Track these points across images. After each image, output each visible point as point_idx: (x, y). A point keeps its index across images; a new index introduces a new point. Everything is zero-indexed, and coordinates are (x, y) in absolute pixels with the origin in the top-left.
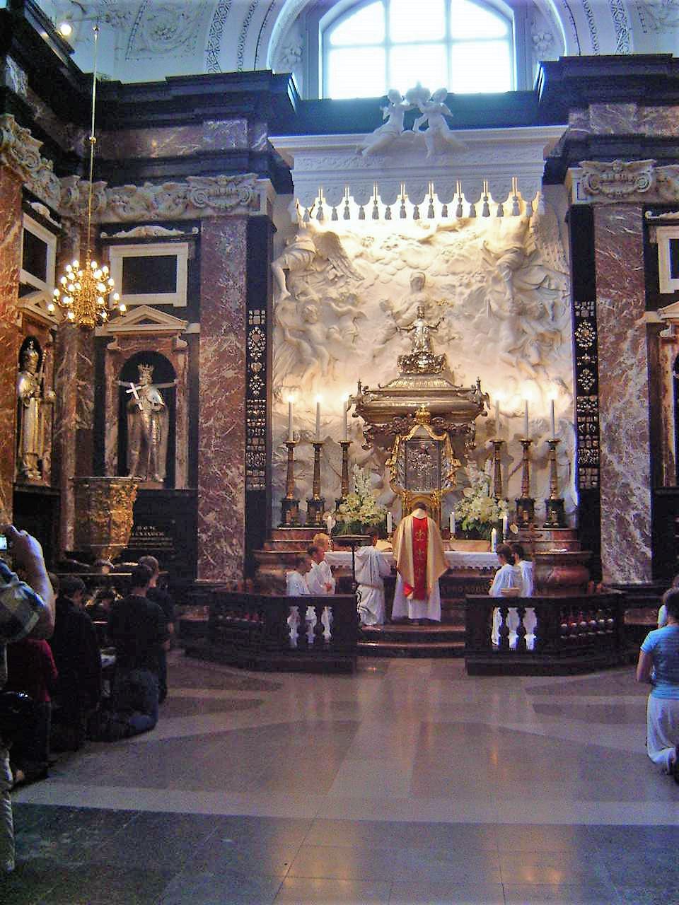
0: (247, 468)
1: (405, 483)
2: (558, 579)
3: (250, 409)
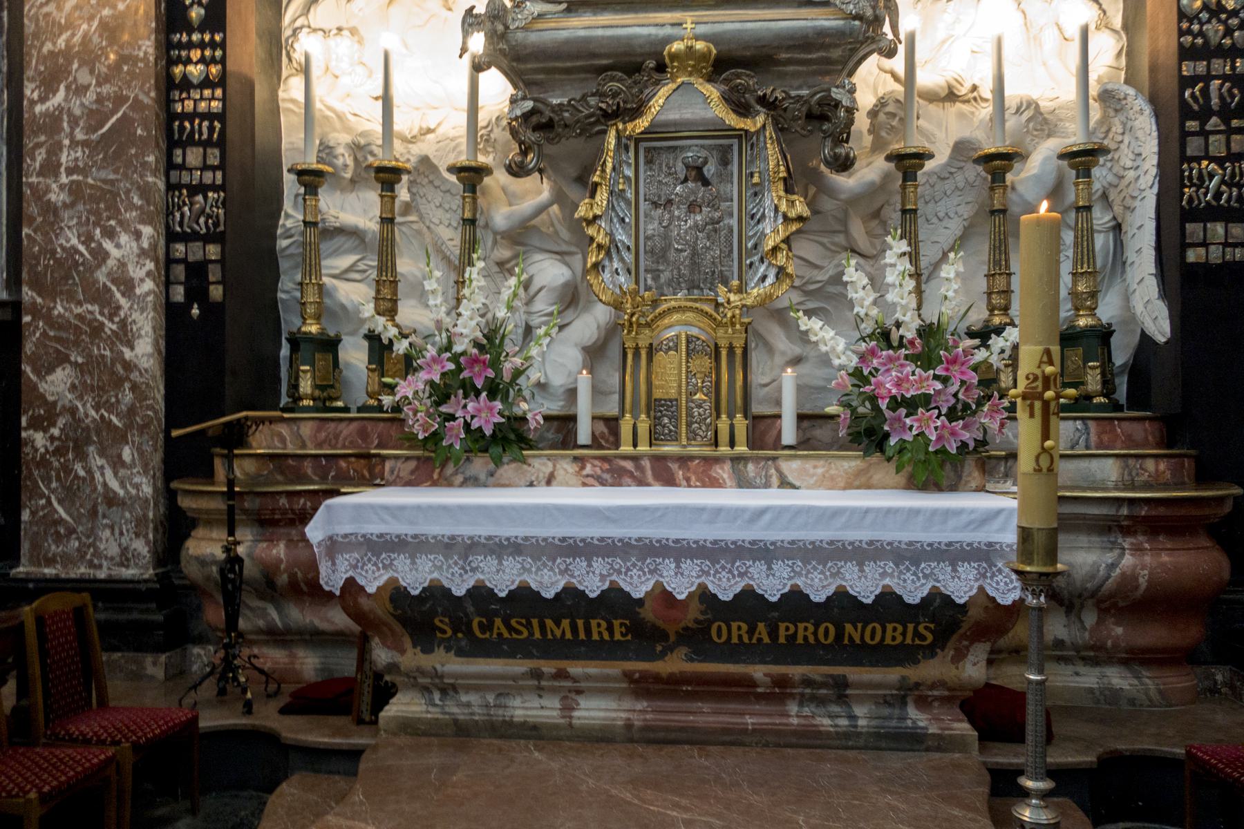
0: (172, 237)
1: (634, 272)
2: (1143, 582)
3: (179, 60)
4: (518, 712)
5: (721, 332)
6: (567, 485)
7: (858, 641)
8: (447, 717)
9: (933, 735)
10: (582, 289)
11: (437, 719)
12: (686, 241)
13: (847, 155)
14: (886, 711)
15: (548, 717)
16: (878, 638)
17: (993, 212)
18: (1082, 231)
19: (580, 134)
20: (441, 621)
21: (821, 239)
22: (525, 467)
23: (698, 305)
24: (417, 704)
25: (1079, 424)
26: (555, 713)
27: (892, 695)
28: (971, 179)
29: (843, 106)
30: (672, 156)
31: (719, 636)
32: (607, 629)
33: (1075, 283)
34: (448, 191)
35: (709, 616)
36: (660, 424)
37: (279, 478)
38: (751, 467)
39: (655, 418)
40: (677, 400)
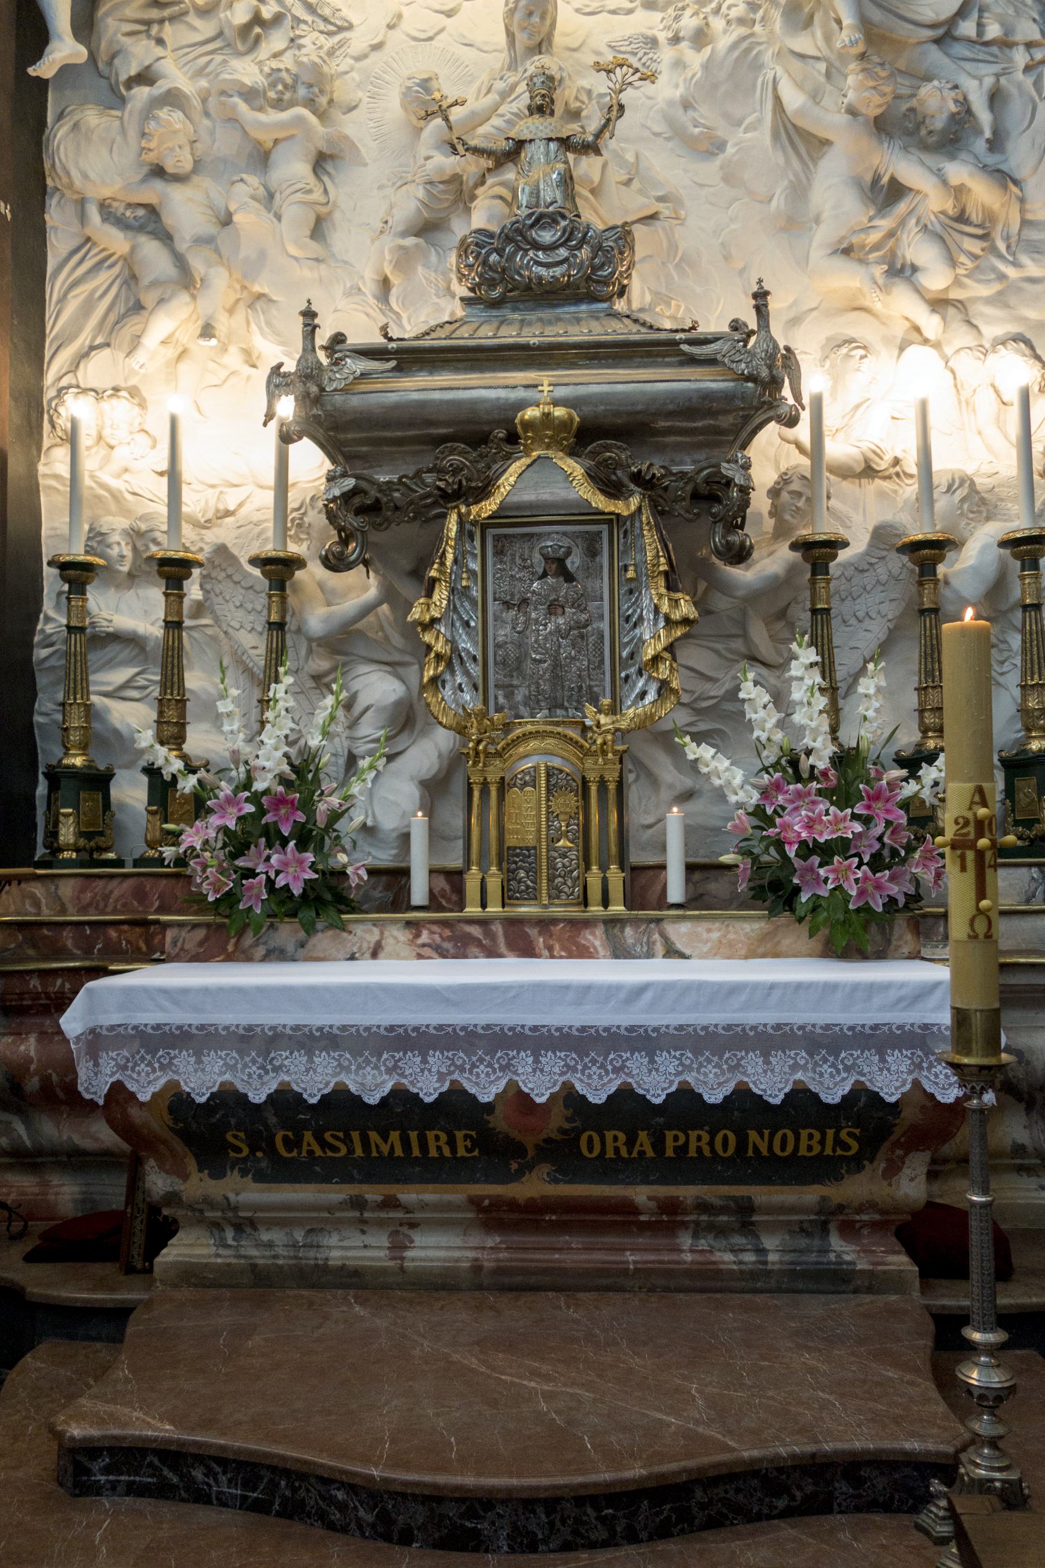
1: (481, 687)
4: (335, 1254)
5: (589, 762)
6: (398, 957)
7: (765, 1152)
8: (243, 1261)
9: (860, 1271)
10: (420, 709)
11: (229, 1265)
12: (546, 649)
13: (742, 544)
14: (803, 1242)
15: (373, 1259)
16: (790, 1149)
17: (922, 612)
18: (1031, 634)
19: (414, 519)
20: (236, 1137)
21: (712, 645)
22: (345, 935)
23: (560, 729)
24: (202, 1245)
25: (1035, 872)
26: (382, 1254)
27: (811, 1221)
28: (896, 571)
29: (736, 485)
30: (526, 545)
31: (591, 1149)
32: (447, 1143)
33: (1024, 698)
34: (251, 587)
35: (578, 1124)
36: (514, 879)
37: (31, 952)
38: (629, 931)
39: (508, 871)
40: (535, 848)
